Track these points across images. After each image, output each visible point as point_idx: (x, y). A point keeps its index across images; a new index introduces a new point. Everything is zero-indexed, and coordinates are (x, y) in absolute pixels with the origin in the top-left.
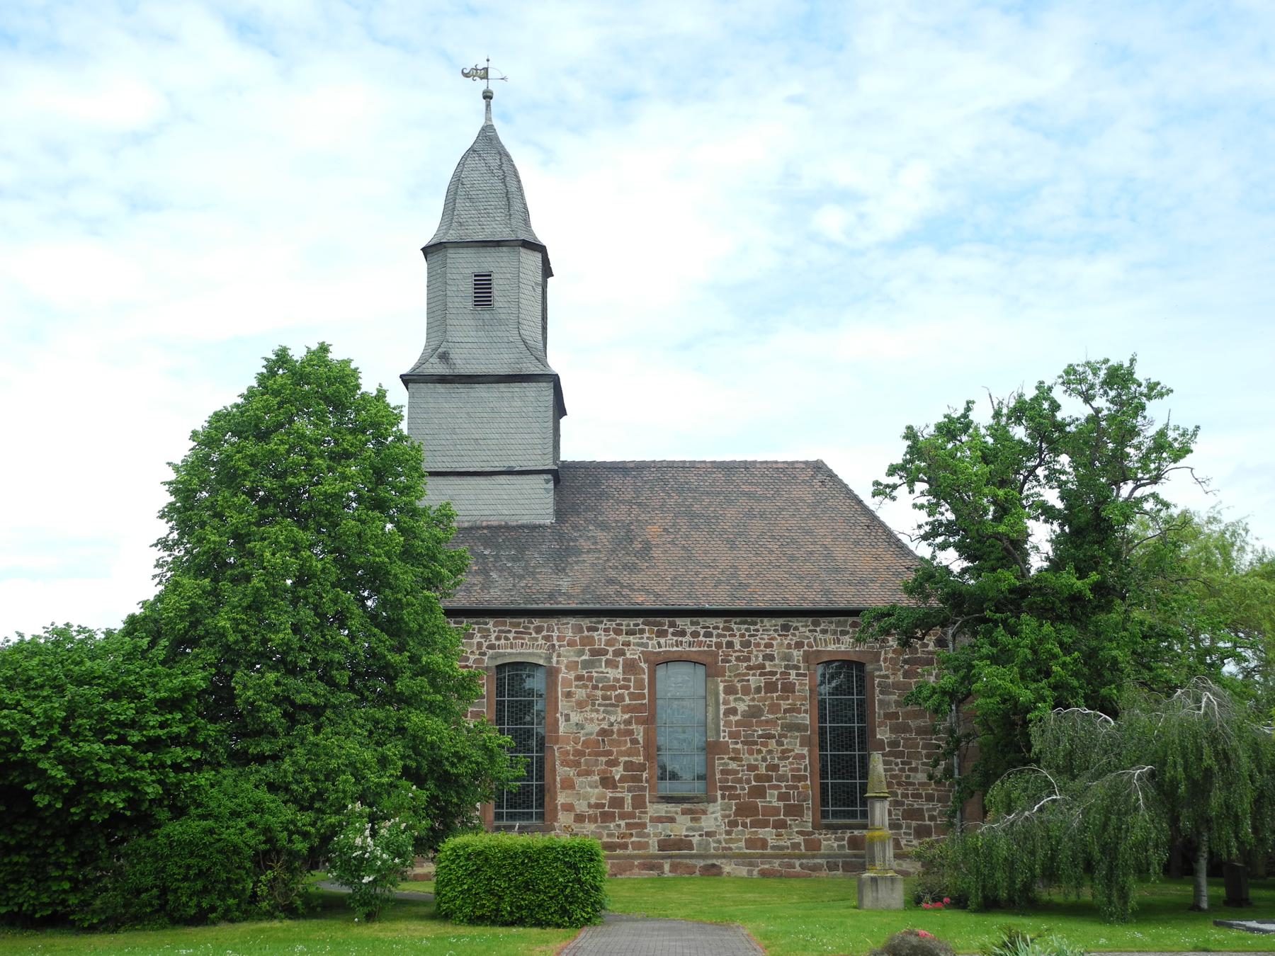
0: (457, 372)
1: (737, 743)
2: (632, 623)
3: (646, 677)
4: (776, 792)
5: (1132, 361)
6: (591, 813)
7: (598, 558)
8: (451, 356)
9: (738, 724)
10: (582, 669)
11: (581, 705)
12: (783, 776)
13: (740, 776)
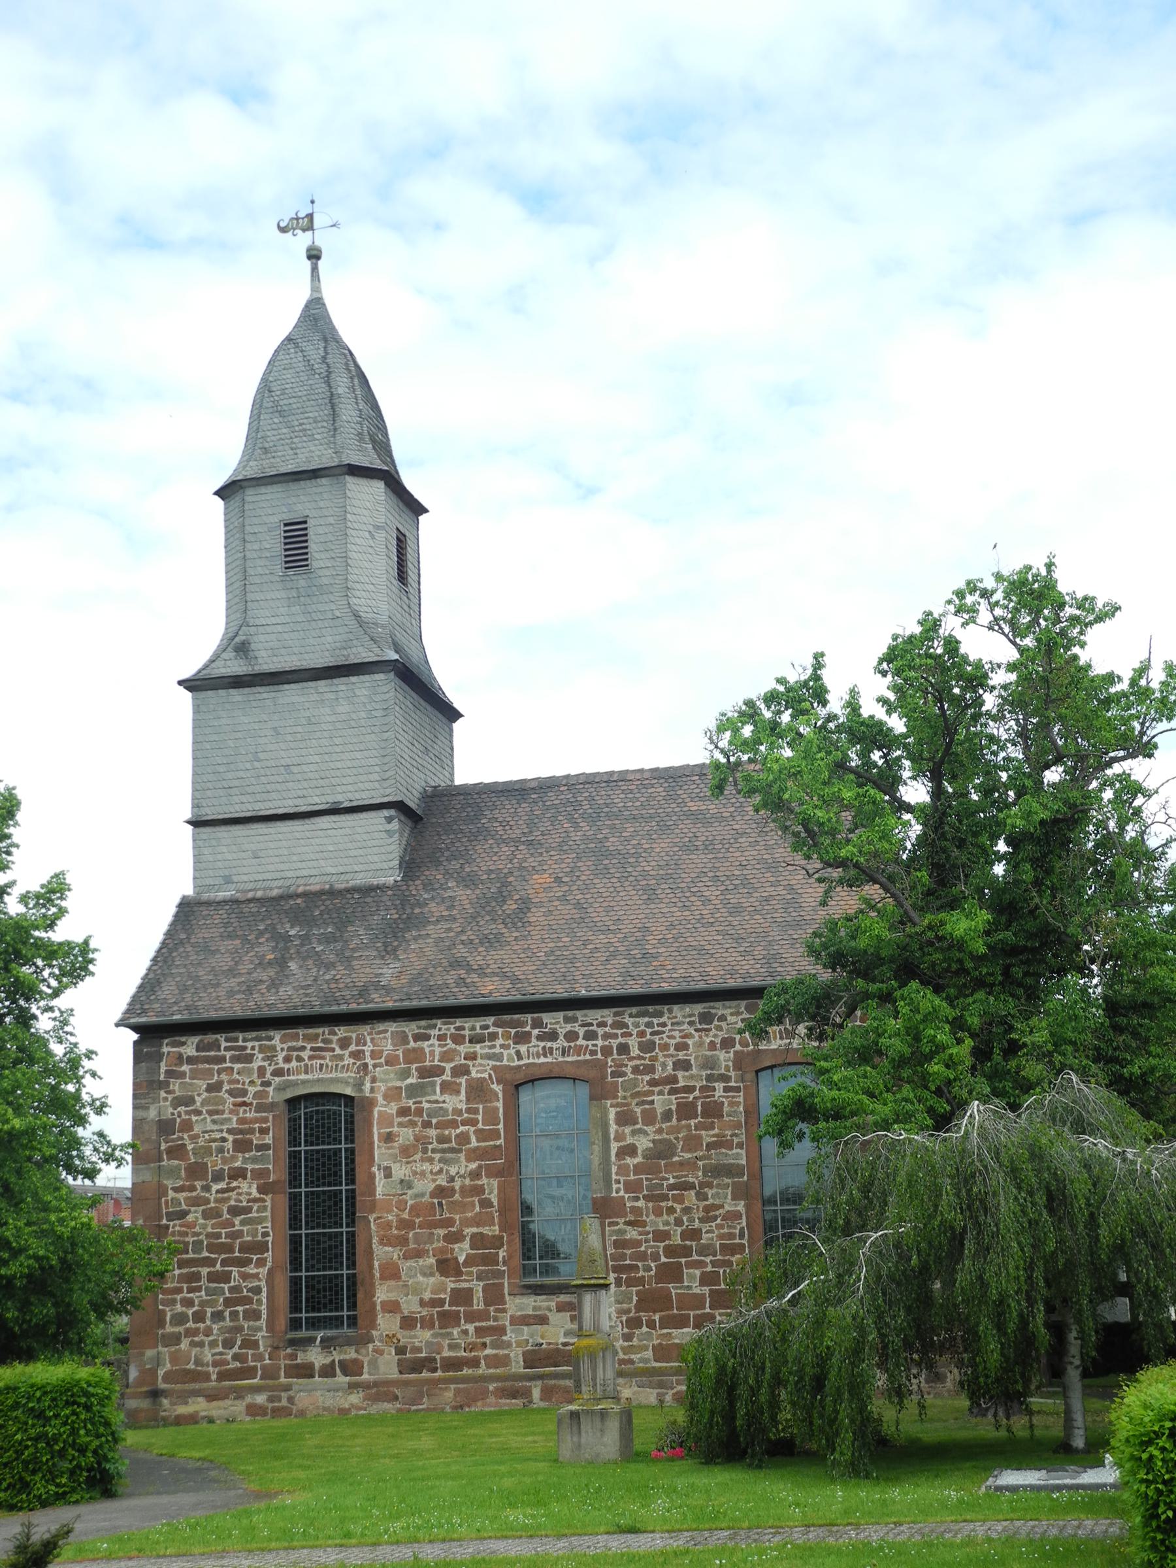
0: (258, 669)
1: (637, 1199)
2: (478, 1025)
3: (500, 1105)
4: (698, 1272)
5: (1050, 566)
6: (424, 1313)
7: (450, 930)
8: (253, 646)
9: (638, 1169)
10: (408, 1097)
11: (406, 1152)
12: (708, 1246)
13: (643, 1249)
